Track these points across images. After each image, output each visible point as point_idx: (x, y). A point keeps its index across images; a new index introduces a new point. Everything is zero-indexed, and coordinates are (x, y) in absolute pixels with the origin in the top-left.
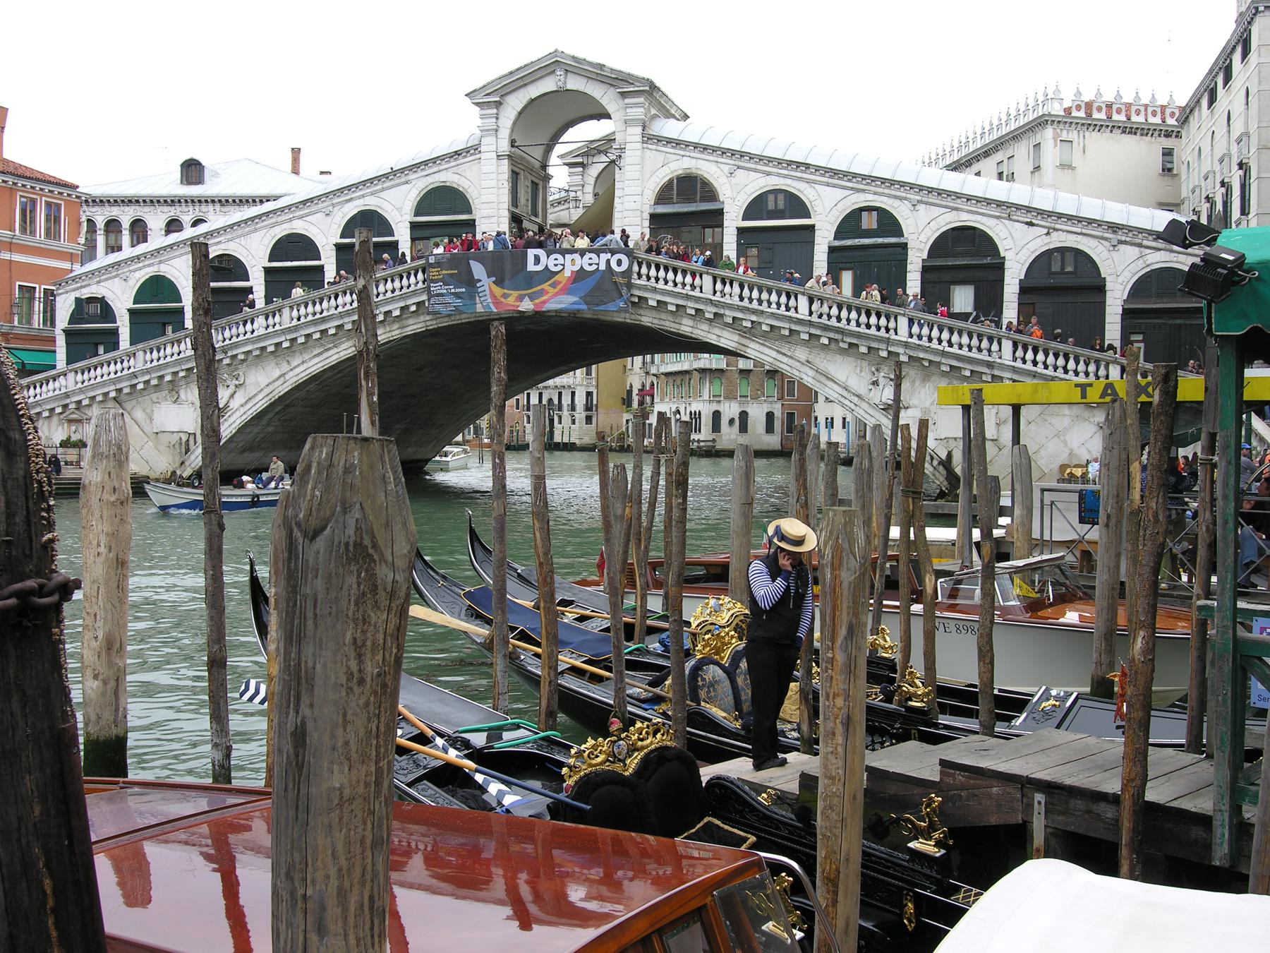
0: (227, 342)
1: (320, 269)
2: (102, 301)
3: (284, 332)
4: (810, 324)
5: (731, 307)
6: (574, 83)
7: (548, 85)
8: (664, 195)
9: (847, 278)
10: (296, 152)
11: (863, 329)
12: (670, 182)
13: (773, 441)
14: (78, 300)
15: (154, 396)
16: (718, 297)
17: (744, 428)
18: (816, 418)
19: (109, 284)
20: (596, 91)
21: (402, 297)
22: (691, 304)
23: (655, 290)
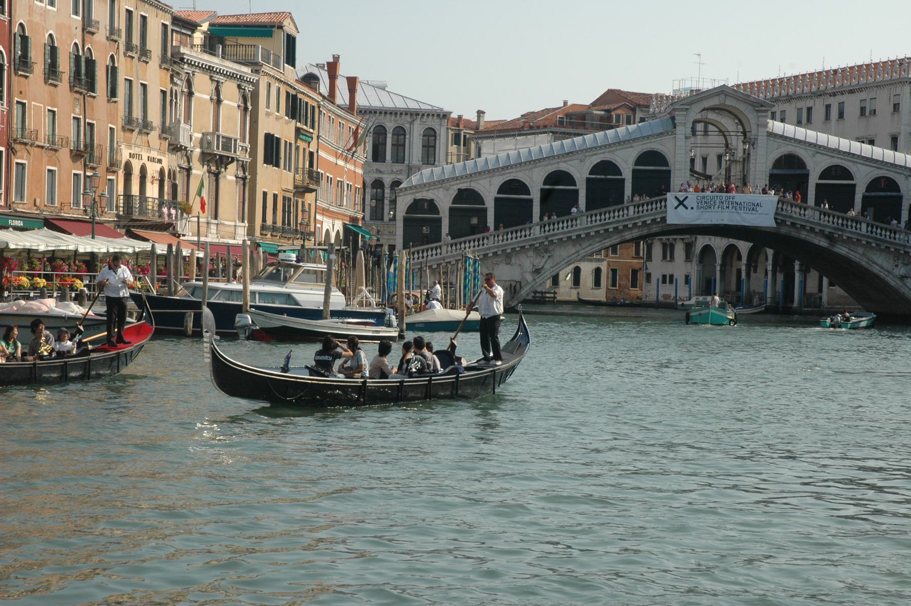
0: (547, 233)
1: (576, 192)
2: (431, 202)
3: (584, 229)
4: (869, 237)
5: (829, 227)
6: (730, 102)
7: (715, 102)
8: (778, 163)
9: (871, 211)
10: (336, 59)
11: (892, 240)
12: (781, 157)
13: (600, 295)
14: (415, 199)
15: (494, 261)
16: (822, 222)
17: (576, 281)
18: (649, 276)
19: (436, 191)
20: (742, 107)
21: (655, 214)
22: (808, 225)
23: (791, 217)
